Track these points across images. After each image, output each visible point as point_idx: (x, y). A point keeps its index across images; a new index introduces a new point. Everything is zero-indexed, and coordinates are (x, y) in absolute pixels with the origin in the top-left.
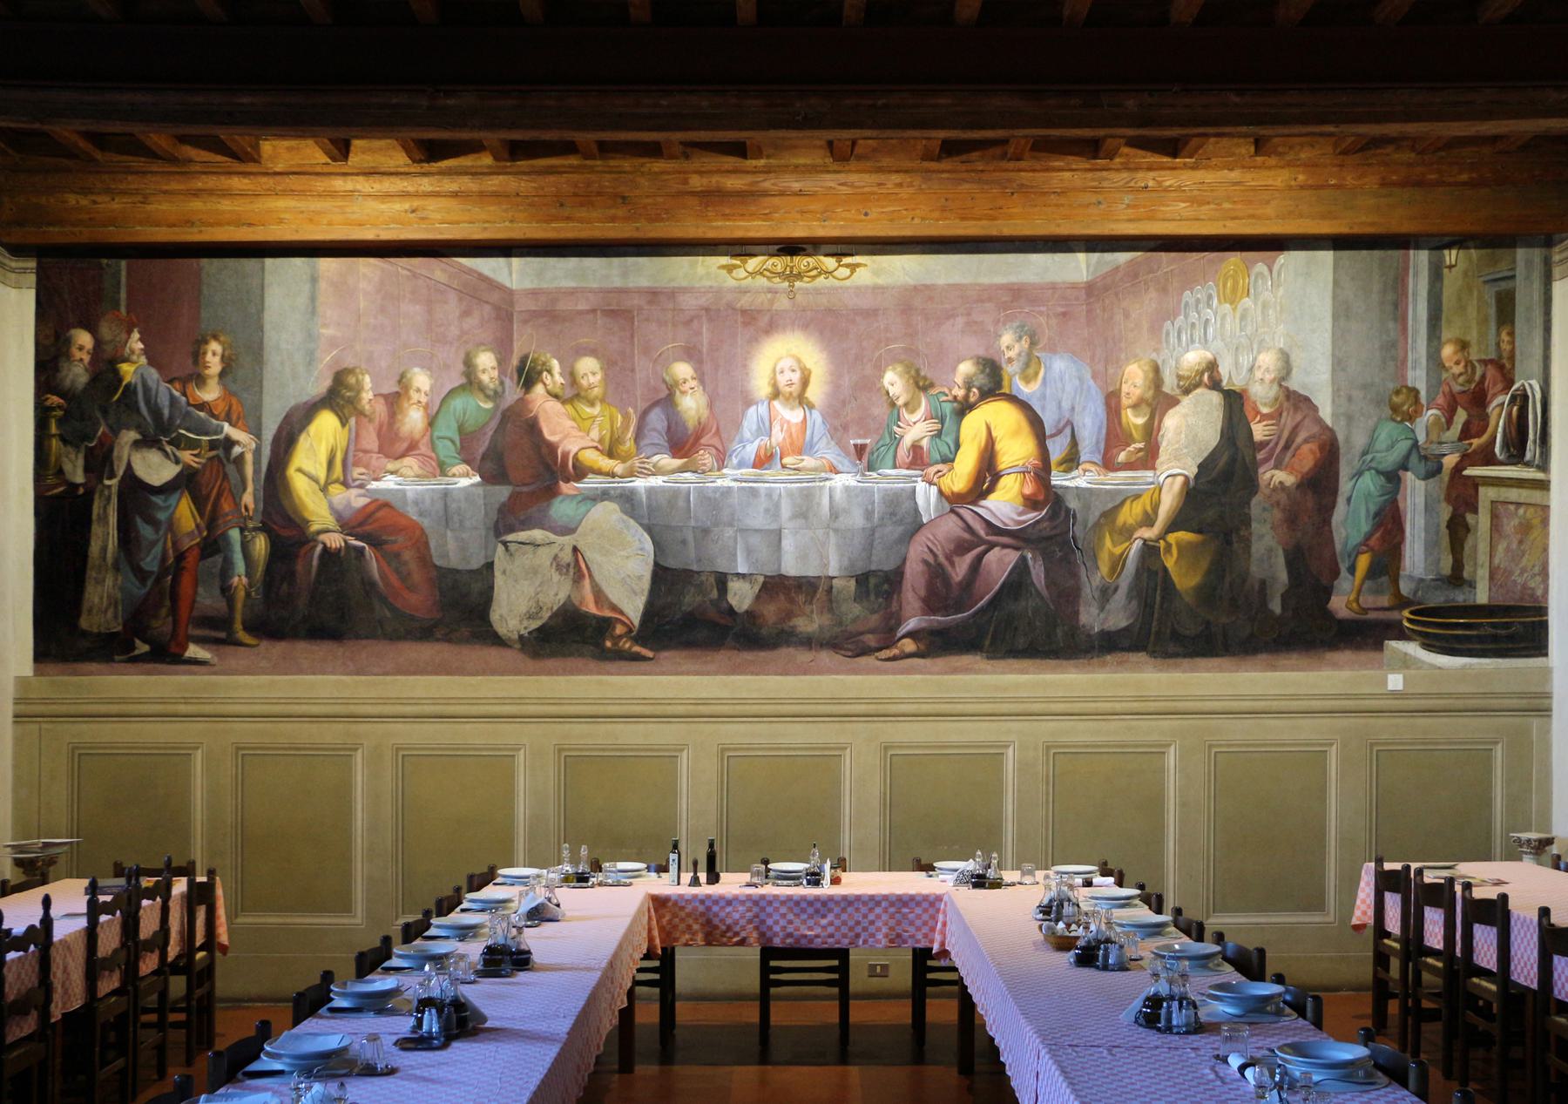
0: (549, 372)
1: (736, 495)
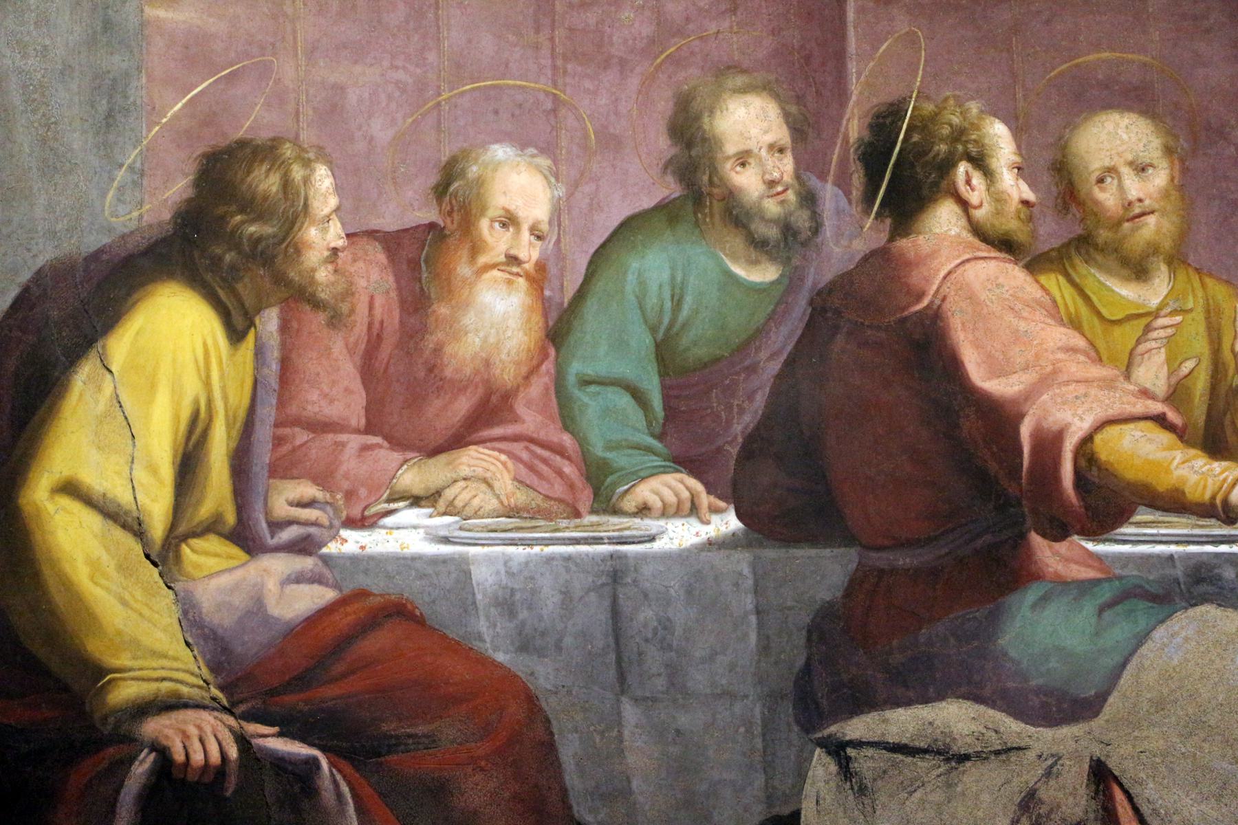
0: (980, 162)
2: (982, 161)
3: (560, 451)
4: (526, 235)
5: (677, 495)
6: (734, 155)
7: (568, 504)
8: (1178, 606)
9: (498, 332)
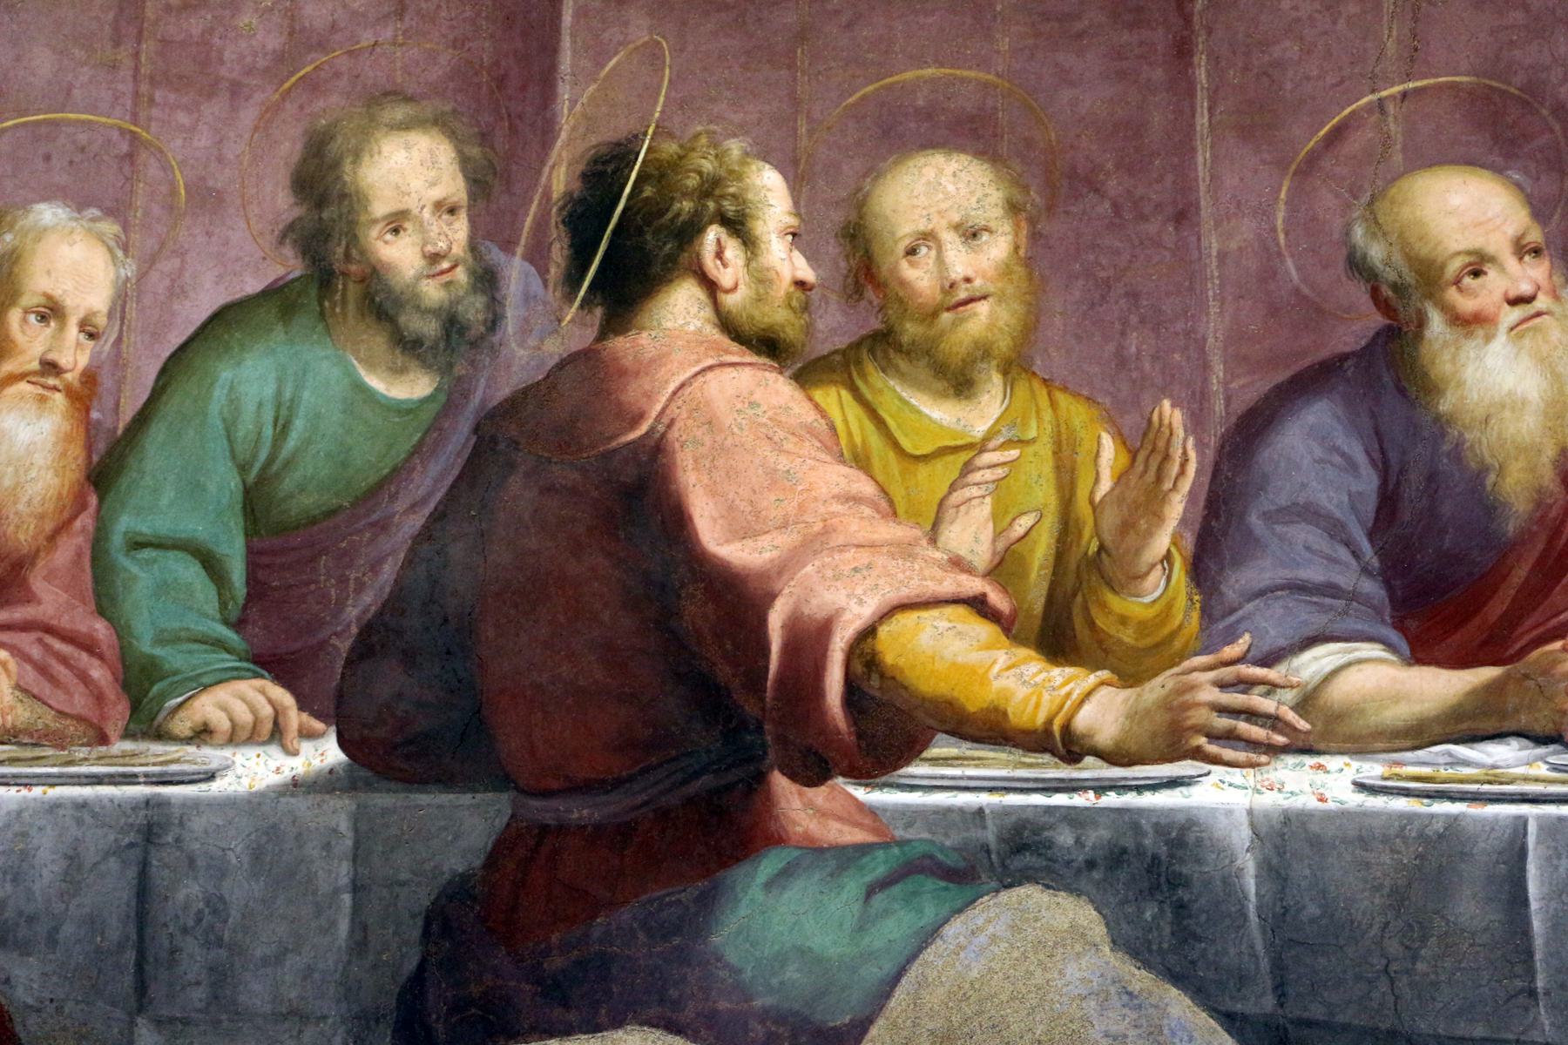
0: (738, 225)
2: (743, 224)
3: (88, 645)
4: (72, 331)
5: (253, 710)
6: (385, 218)
7: (90, 724)
8: (985, 887)
9: (17, 471)
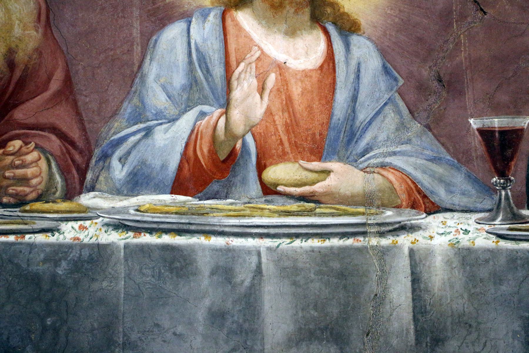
1: (122, 269)
